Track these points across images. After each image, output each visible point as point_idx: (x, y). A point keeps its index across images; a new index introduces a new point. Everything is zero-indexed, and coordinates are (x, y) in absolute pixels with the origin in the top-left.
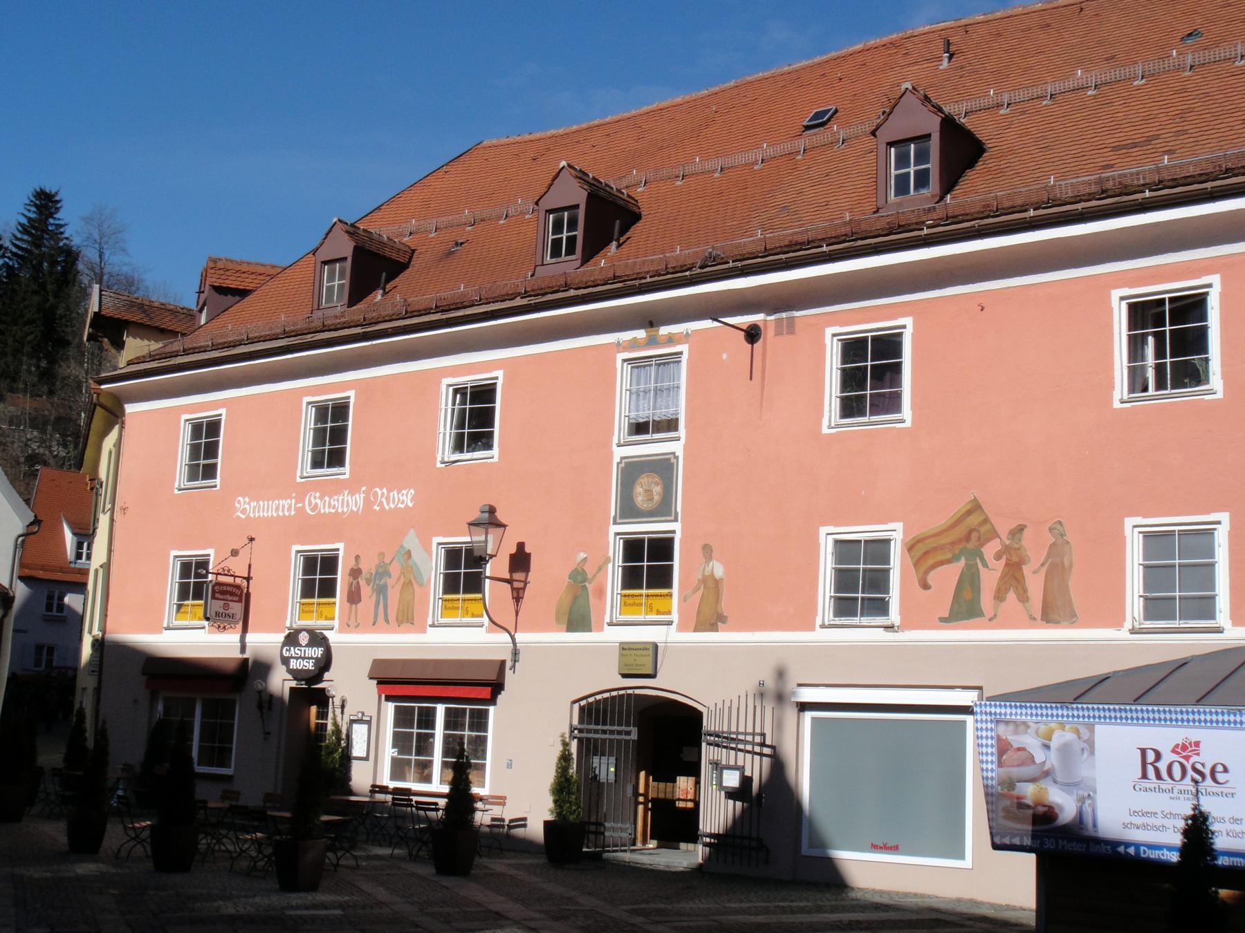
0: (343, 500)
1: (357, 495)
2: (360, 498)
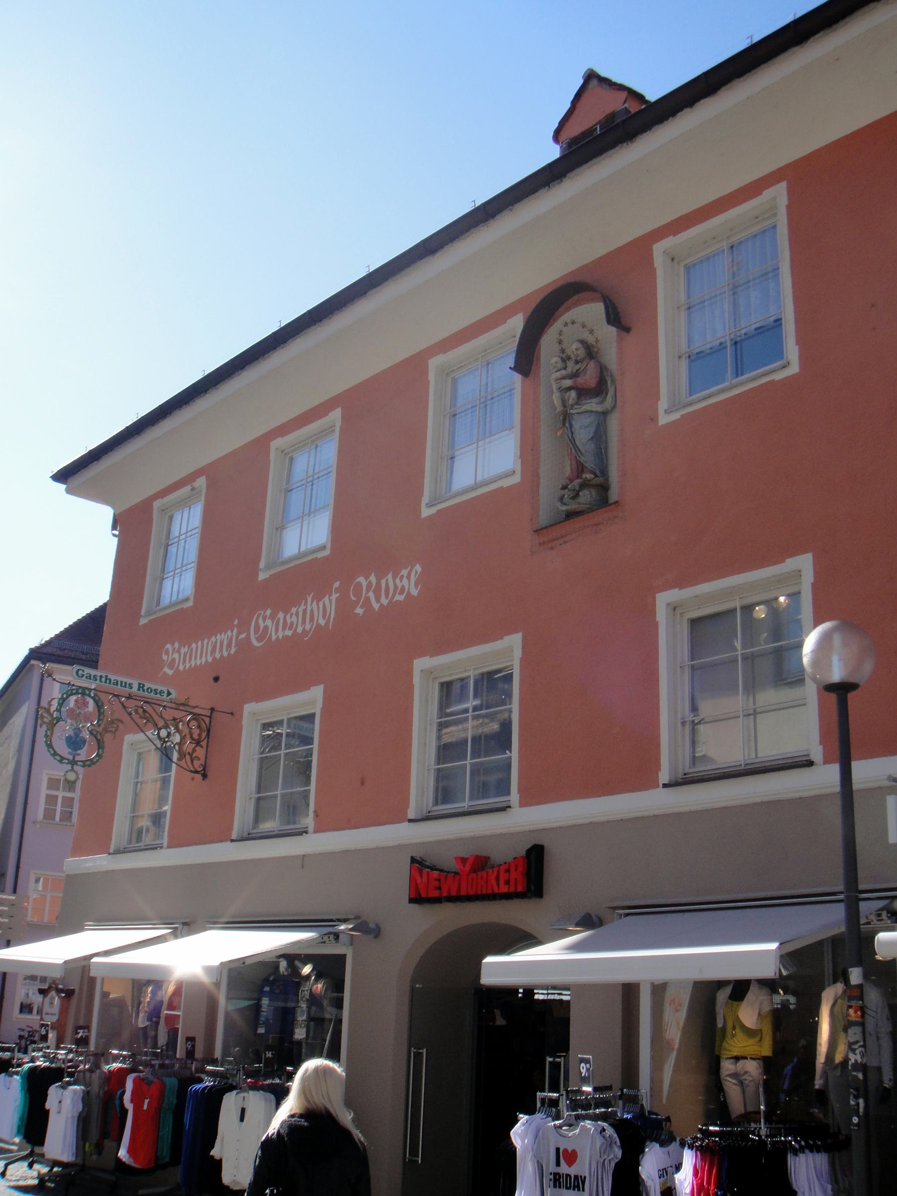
0: (305, 611)
1: (326, 599)
2: (330, 602)
